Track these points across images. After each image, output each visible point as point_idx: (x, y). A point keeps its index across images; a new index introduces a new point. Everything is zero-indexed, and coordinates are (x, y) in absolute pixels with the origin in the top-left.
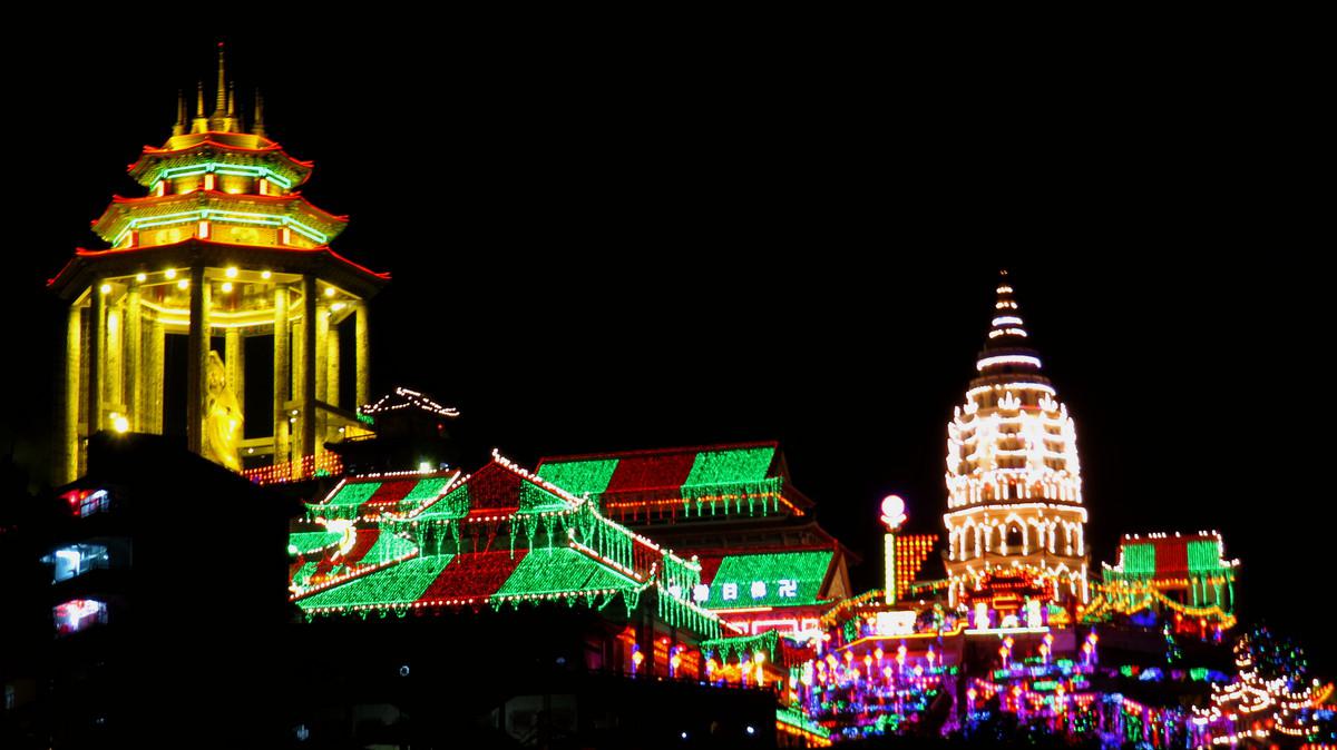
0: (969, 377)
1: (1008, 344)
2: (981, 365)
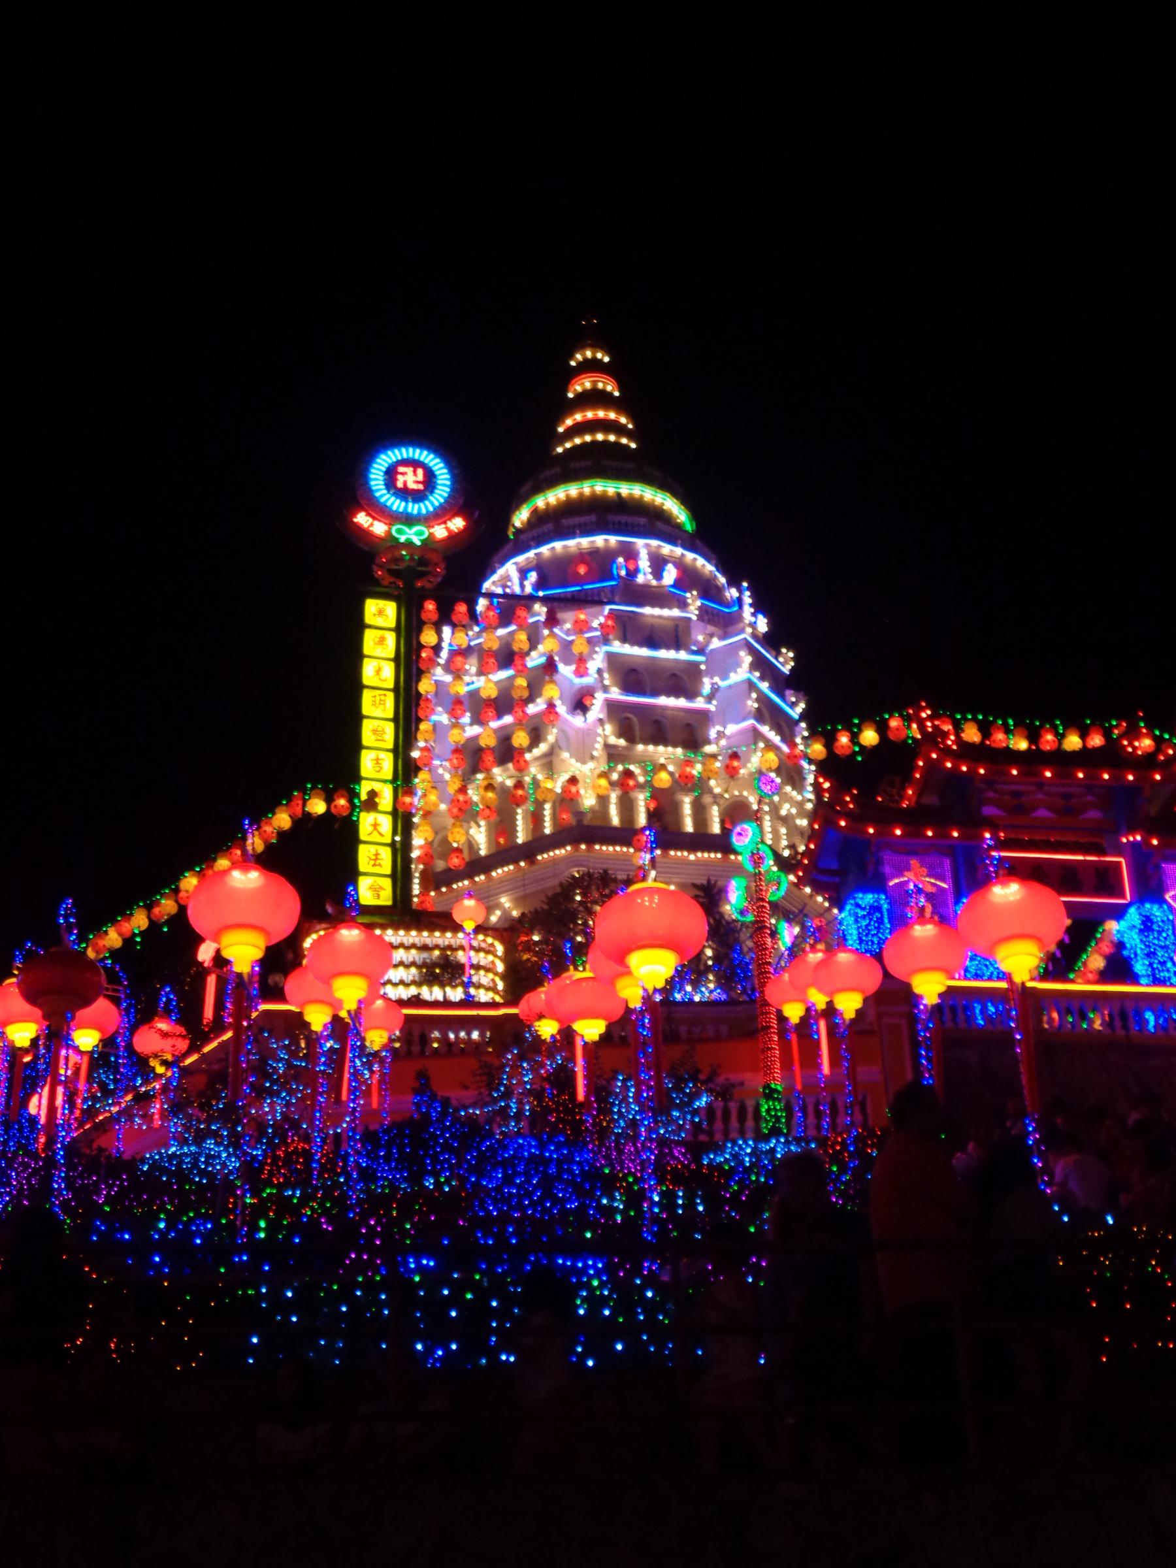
2: (521, 517)
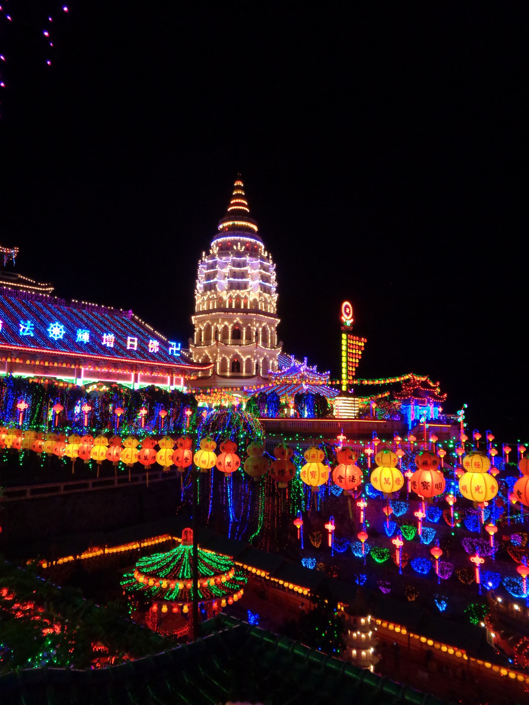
0: (215, 233)
1: (238, 215)
2: (221, 227)
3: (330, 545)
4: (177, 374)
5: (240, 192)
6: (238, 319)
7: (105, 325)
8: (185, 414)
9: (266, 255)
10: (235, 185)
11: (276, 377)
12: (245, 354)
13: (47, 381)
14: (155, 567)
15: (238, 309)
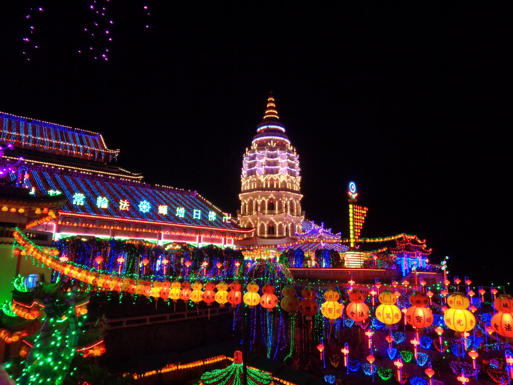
0: (255, 134)
2: (259, 130)
3: (346, 365)
4: (229, 236)
5: (272, 105)
6: (272, 195)
7: (178, 202)
8: (235, 266)
9: (292, 148)
10: (269, 100)
11: (301, 238)
12: (278, 220)
13: (138, 242)
14: (215, 380)
15: (272, 188)
